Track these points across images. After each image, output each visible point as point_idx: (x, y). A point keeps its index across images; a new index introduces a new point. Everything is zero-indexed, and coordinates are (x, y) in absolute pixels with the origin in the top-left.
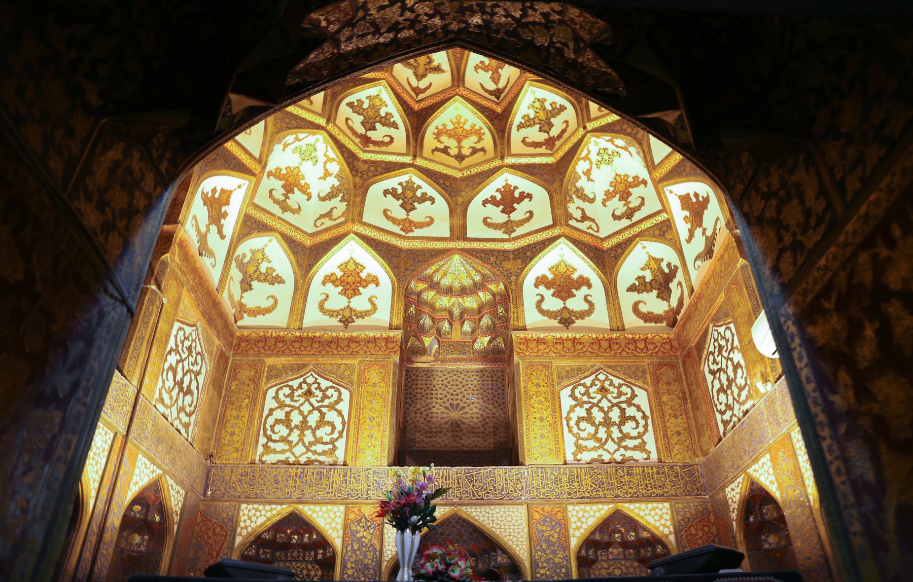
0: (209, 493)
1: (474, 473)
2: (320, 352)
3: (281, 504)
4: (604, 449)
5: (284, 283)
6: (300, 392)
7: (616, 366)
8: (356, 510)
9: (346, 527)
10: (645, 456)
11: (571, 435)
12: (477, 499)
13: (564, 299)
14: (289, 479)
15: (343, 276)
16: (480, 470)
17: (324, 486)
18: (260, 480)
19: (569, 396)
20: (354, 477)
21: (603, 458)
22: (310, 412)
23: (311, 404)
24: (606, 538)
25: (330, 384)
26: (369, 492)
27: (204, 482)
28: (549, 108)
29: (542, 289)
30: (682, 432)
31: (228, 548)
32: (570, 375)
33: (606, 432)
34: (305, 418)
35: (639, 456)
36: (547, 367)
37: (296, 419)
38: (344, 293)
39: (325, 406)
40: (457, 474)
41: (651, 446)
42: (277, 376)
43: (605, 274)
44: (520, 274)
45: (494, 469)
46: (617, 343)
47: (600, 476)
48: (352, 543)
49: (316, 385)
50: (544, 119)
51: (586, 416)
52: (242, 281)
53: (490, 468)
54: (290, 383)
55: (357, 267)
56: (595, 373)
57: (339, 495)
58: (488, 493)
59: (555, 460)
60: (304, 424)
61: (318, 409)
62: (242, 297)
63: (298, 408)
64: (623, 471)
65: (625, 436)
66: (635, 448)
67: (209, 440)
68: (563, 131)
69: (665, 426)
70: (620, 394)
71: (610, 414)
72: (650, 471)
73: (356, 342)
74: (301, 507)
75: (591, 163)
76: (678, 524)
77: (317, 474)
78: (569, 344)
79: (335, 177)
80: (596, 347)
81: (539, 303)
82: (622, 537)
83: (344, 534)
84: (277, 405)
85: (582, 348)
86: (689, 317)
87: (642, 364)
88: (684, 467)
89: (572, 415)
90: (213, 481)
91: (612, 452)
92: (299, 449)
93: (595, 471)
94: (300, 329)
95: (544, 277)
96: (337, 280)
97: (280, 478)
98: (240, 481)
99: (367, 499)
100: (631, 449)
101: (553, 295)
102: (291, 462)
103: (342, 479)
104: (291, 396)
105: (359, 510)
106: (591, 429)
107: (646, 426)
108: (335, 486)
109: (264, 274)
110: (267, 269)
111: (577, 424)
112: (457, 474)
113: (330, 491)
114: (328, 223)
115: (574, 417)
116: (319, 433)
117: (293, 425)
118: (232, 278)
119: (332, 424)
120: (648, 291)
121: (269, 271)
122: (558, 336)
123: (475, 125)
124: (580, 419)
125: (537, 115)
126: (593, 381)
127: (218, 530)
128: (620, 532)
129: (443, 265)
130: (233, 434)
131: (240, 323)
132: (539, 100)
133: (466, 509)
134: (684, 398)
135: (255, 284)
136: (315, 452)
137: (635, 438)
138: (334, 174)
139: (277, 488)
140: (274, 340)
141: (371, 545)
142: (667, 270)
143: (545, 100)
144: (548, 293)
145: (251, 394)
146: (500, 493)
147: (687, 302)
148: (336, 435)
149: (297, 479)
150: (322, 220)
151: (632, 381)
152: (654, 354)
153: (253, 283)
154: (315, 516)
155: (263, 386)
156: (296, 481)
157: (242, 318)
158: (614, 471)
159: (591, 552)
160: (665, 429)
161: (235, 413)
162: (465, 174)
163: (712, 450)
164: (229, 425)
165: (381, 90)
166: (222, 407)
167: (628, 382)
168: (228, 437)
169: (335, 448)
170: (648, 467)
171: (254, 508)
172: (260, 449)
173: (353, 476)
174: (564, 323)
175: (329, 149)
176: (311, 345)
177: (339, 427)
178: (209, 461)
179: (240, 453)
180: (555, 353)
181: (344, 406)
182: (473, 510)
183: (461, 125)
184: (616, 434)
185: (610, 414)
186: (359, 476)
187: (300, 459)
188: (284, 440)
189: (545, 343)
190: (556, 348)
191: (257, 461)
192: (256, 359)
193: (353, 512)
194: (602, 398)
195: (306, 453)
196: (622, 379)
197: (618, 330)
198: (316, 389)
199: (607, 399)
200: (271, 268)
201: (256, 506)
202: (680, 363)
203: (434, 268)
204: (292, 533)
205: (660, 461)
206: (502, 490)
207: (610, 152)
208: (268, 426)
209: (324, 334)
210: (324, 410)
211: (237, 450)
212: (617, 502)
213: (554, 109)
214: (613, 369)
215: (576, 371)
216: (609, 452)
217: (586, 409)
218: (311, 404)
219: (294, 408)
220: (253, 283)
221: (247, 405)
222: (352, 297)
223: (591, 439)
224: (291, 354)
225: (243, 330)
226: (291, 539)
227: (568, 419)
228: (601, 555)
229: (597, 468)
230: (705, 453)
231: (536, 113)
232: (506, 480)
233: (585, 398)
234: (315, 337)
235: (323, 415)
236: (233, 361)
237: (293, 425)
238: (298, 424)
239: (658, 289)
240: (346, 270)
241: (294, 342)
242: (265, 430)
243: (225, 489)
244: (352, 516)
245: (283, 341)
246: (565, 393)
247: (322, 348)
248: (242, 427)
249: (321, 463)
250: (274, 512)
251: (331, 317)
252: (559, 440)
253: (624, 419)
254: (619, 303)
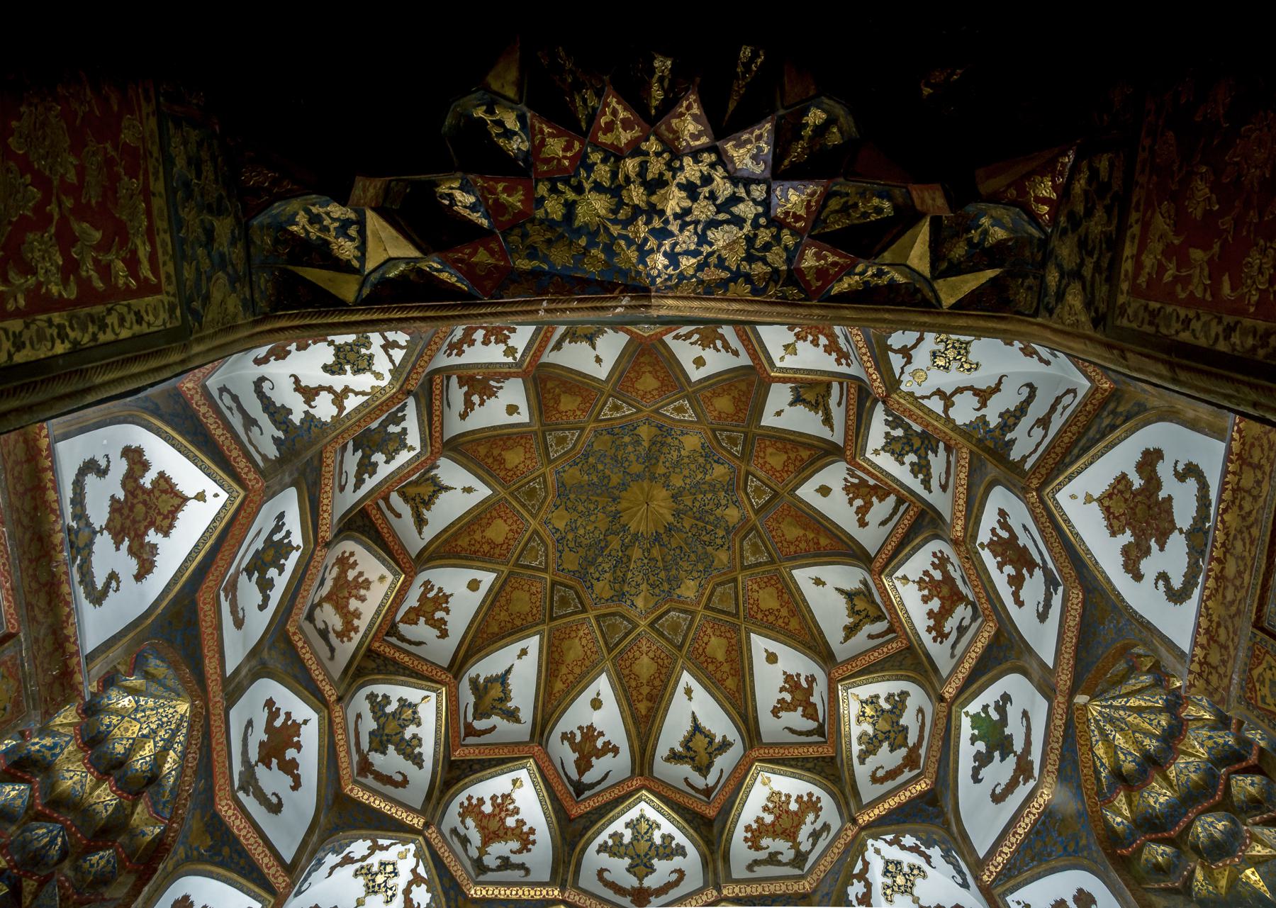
28: (408, 734)
38: (116, 507)
50: (387, 731)
55: (166, 517)
68: (387, 780)
73: (49, 603)
75: (364, 858)
79: (306, 413)
96: (136, 480)
114: (237, 421)
123: (358, 617)
125: (391, 717)
132: (415, 713)
138: (312, 411)
143: (419, 724)
150: (234, 406)
162: (296, 638)
165: (414, 449)
175: (362, 399)
183: (354, 592)
207: (390, 883)
213: (409, 743)
231: (394, 714)
240: (157, 493)
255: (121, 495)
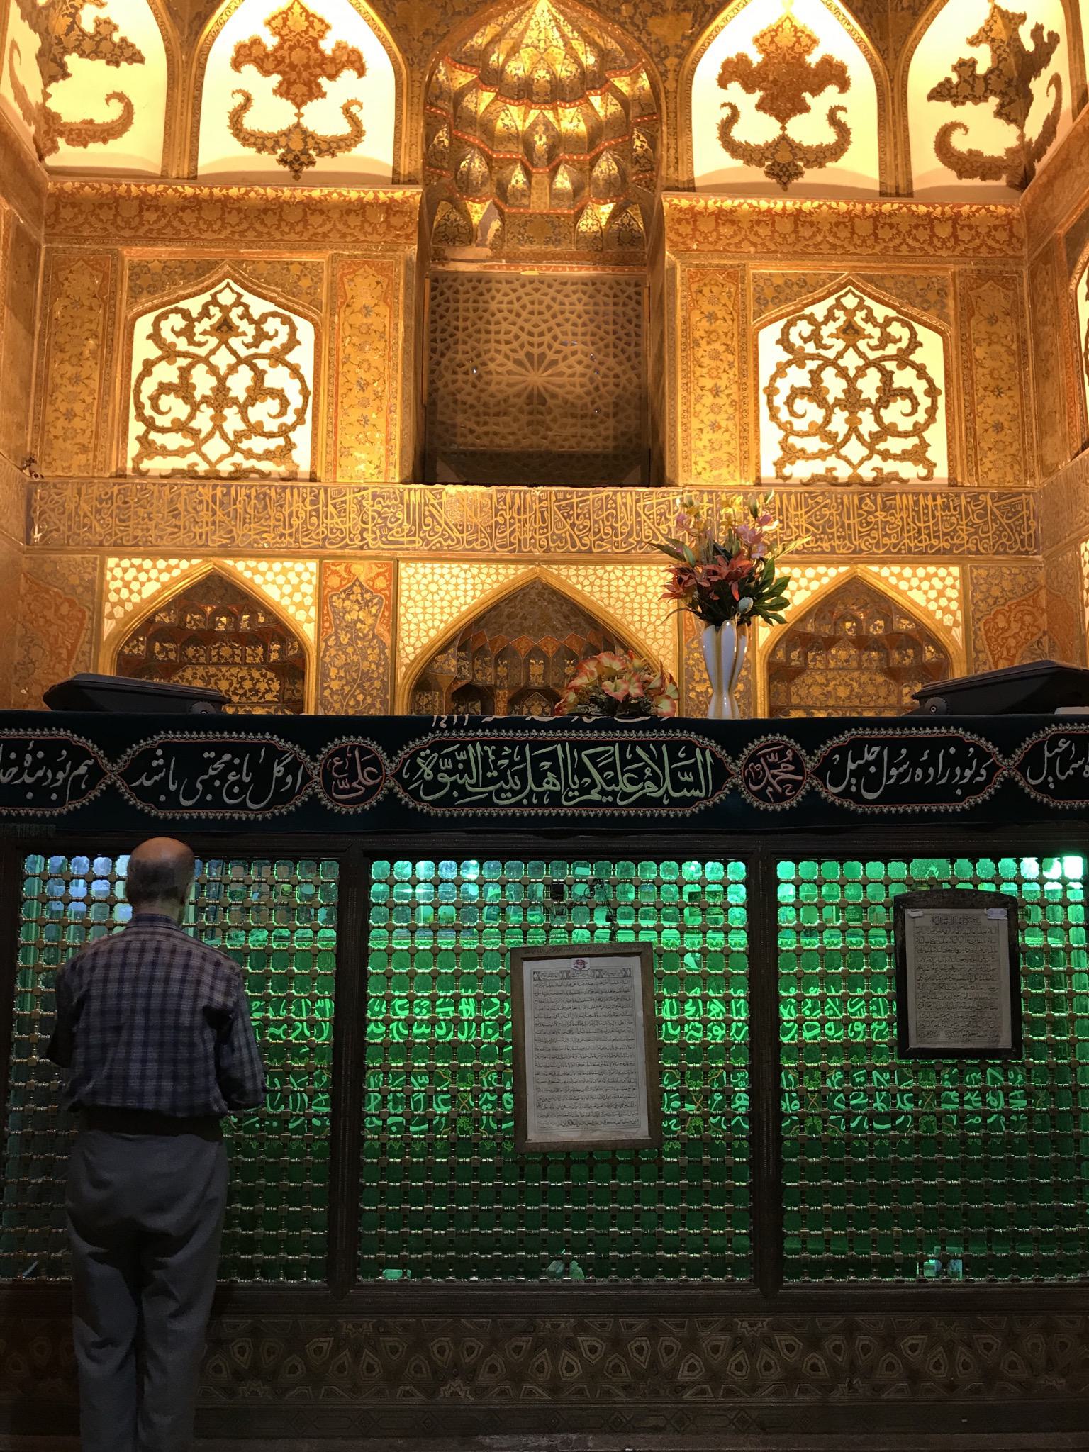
0: (37, 536)
1: (575, 500)
2: (242, 233)
3: (189, 557)
4: (839, 457)
5: (142, 60)
6: (206, 324)
7: (882, 278)
8: (340, 569)
9: (323, 600)
10: (923, 472)
11: (774, 425)
12: (580, 551)
13: (783, 118)
14: (199, 508)
15: (280, 47)
16: (587, 494)
17: (272, 522)
18: (141, 512)
19: (778, 342)
20: (334, 505)
21: (835, 473)
22: (232, 369)
23: (233, 352)
24: (827, 630)
25: (271, 307)
26: (365, 535)
27: (23, 516)
29: (735, 90)
30: (1006, 424)
31: (90, 642)
32: (782, 297)
33: (847, 421)
34: (222, 380)
35: (909, 471)
36: (735, 276)
37: (203, 382)
38: (284, 91)
39: (263, 356)
40: (541, 501)
41: (938, 451)
42: (153, 289)
43: (883, 53)
44: (687, 51)
45: (615, 493)
46: (891, 226)
47: (826, 511)
48: (336, 633)
49: (240, 310)
51: (809, 385)
52: (41, 56)
53: (608, 491)
54: (183, 304)
55: (311, 24)
56: (836, 291)
57: (306, 540)
58: (602, 540)
59: (737, 475)
60: (220, 398)
61: (248, 361)
62: (47, 96)
63: (206, 360)
64: (875, 502)
65: (888, 431)
66: (904, 456)
67: (21, 427)
69: (972, 412)
70: (886, 340)
71: (860, 384)
72: (930, 503)
73: (322, 212)
74: (229, 562)
76: (972, 608)
77: (256, 497)
78: (786, 226)
80: (844, 233)
81: (726, 127)
82: (858, 628)
83: (320, 614)
84: (159, 353)
85: (814, 236)
86: (1064, 163)
87: (941, 274)
88: (1001, 496)
89: (779, 383)
90: (42, 513)
91: (855, 462)
92: (216, 448)
93: (820, 499)
94: (193, 177)
95: (742, 59)
96: (267, 55)
97: (181, 507)
98: (99, 511)
99: (361, 548)
100: (896, 457)
101: (759, 107)
102: (201, 474)
103: (309, 508)
104: (188, 332)
105: (348, 570)
106: (817, 414)
107: (932, 411)
108: (295, 522)
109: (92, 37)
110: (98, 23)
111: (789, 402)
112: (541, 501)
113: (287, 532)
115: (784, 386)
116: (255, 413)
117: (831, 400)
118: (14, 45)
119: (279, 394)
120: (977, 99)
121: (104, 30)
122: (764, 204)
124: (796, 393)
126: (830, 310)
127: (65, 609)
128: (855, 619)
129: (511, 25)
130: (70, 415)
131: (51, 161)
133: (559, 570)
134: (1022, 354)
135: (72, 60)
136: (249, 454)
137: (906, 435)
139: (176, 526)
140: (136, 202)
141: (374, 636)
142: (1029, 46)
144: (747, 101)
145: (100, 329)
146: (625, 541)
147: (1064, 128)
148: (290, 418)
149: (217, 508)
151: (915, 312)
152: (971, 253)
153: (67, 59)
154: (258, 580)
155: (124, 312)
156: (214, 513)
157: (55, 148)
158: (856, 501)
159: (794, 654)
160: (972, 417)
161: (69, 369)
163: (1066, 464)
164: (61, 397)
166: (40, 357)
167: (906, 315)
168: (61, 422)
169: (290, 446)
170: (926, 494)
171: (132, 566)
172: (133, 448)
173: (330, 502)
174: (780, 177)
176: (223, 219)
177: (296, 401)
178: (27, 472)
179: (91, 455)
180: (755, 245)
181: (303, 356)
182: (572, 572)
184: (868, 424)
185: (860, 384)
186: (343, 502)
187: (219, 467)
188: (180, 427)
189: (733, 222)
190: (756, 234)
191: (129, 472)
192: (101, 248)
193: (336, 573)
194: (845, 349)
195: (230, 455)
196: (894, 307)
197: (898, 195)
198: (241, 318)
199: (857, 350)
200: (107, 22)
201: (137, 561)
202: (1025, 273)
203: (490, 31)
204: (216, 613)
205: (952, 482)
206: (630, 534)
208: (144, 398)
209: (247, 193)
210: (262, 364)
211: (84, 449)
212: (856, 563)
214: (874, 285)
215: (795, 288)
216: (849, 462)
217: (811, 372)
218: (233, 352)
219: (197, 360)
220: (67, 59)
221: (93, 353)
222: (304, 103)
223: (814, 435)
224: (176, 239)
225: (61, 178)
226: (215, 624)
227: (771, 391)
228: (814, 660)
229: (823, 494)
230: (1048, 471)
232: (638, 515)
233: (810, 348)
234: (227, 197)
235: (259, 375)
236: (48, 251)
237: (198, 396)
238: (209, 393)
239: (1001, 94)
240: (285, 32)
241: (183, 209)
242: (139, 407)
243: (70, 528)
244: (334, 582)
245: (157, 208)
246: (768, 337)
247: (245, 226)
248: (89, 400)
249: (264, 476)
250: (176, 573)
251: (259, 150)
252: (748, 436)
253: (888, 393)
254: (906, 128)
255: (276, 79)
